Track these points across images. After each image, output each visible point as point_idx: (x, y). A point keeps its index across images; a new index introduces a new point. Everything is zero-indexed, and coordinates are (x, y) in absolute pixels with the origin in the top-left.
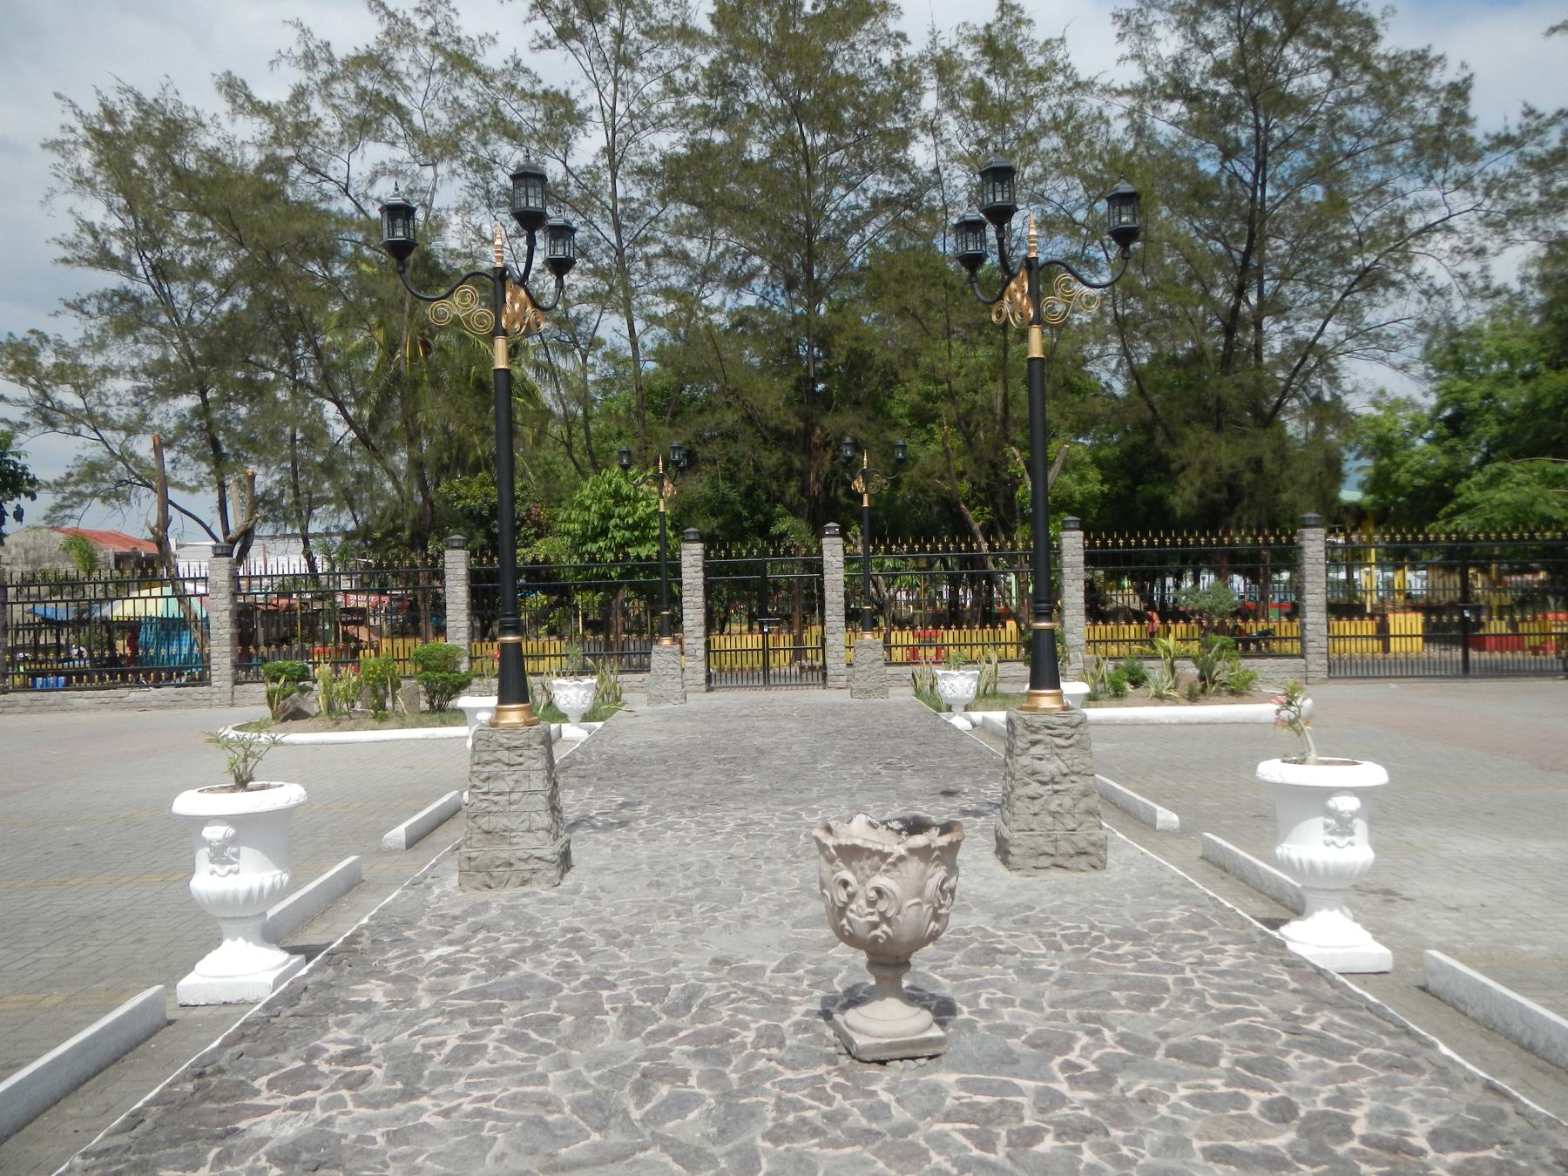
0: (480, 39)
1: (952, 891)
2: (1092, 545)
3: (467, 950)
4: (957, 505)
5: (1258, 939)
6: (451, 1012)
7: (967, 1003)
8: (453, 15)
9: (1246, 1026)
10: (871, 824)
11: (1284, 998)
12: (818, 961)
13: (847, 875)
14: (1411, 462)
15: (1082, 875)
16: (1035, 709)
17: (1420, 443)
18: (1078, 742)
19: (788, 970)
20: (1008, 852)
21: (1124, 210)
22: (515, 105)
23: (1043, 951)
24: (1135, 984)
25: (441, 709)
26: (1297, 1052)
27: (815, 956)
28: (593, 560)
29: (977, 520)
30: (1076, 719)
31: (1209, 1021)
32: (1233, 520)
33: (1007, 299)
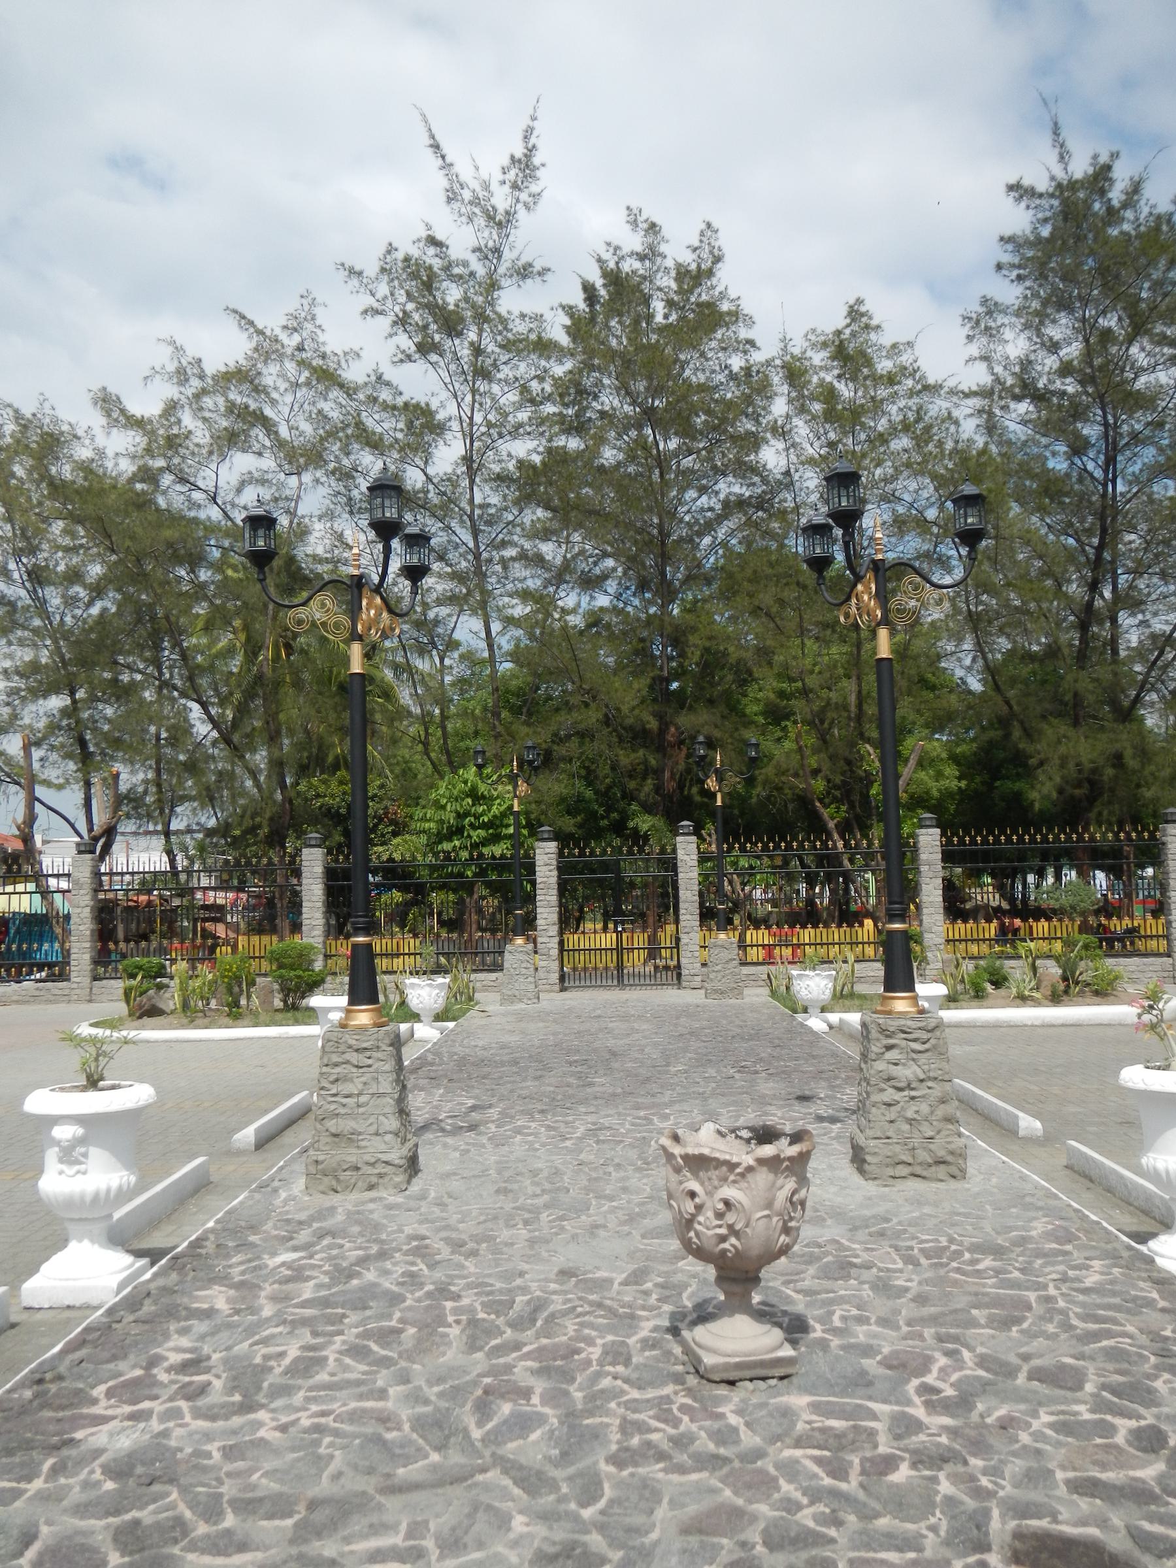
0: (345, 354)
1: (803, 1203)
2: (949, 842)
3: (311, 1257)
5: (1125, 1254)
6: (293, 1322)
7: (820, 1320)
8: (318, 331)
9: (1112, 1348)
10: (719, 1132)
11: (1152, 1318)
12: (667, 1274)
13: (694, 1185)
15: (940, 1185)
16: (890, 1013)
18: (935, 1047)
19: (636, 1283)
20: (864, 1161)
21: (969, 511)
22: (376, 417)
23: (900, 1265)
24: (996, 1302)
25: (295, 1007)
26: (1166, 1376)
27: (665, 1268)
28: (447, 857)
29: (832, 818)
30: (932, 1023)
31: (1074, 1342)
32: (1092, 815)
33: (854, 601)
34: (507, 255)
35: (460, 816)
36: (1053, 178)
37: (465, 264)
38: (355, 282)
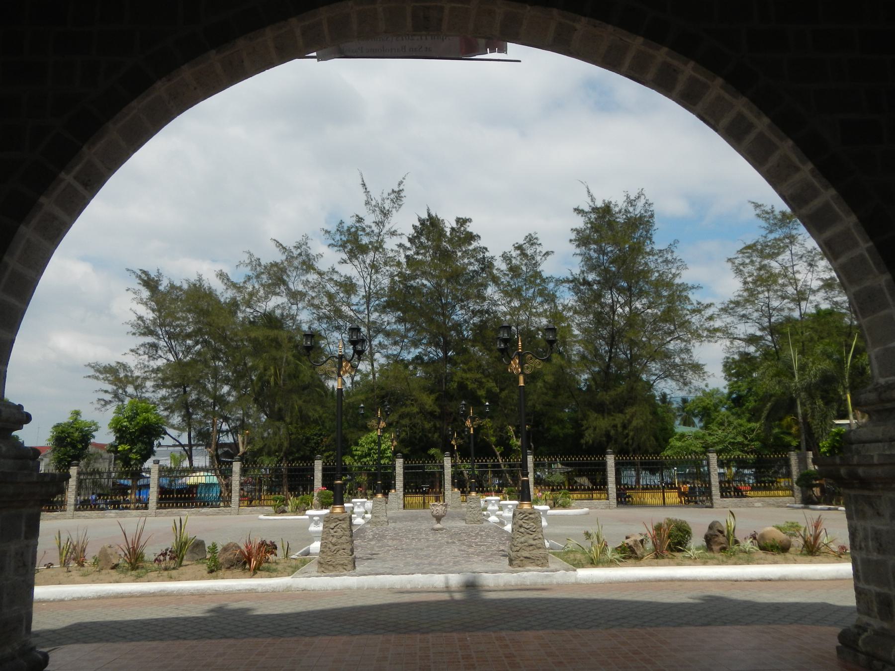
2: (536, 460)
4: (491, 446)
8: (308, 249)
14: (718, 419)
17: (723, 410)
22: (332, 285)
28: (365, 464)
34: (387, 227)
35: (370, 449)
36: (590, 206)
37: (370, 227)
38: (327, 235)
